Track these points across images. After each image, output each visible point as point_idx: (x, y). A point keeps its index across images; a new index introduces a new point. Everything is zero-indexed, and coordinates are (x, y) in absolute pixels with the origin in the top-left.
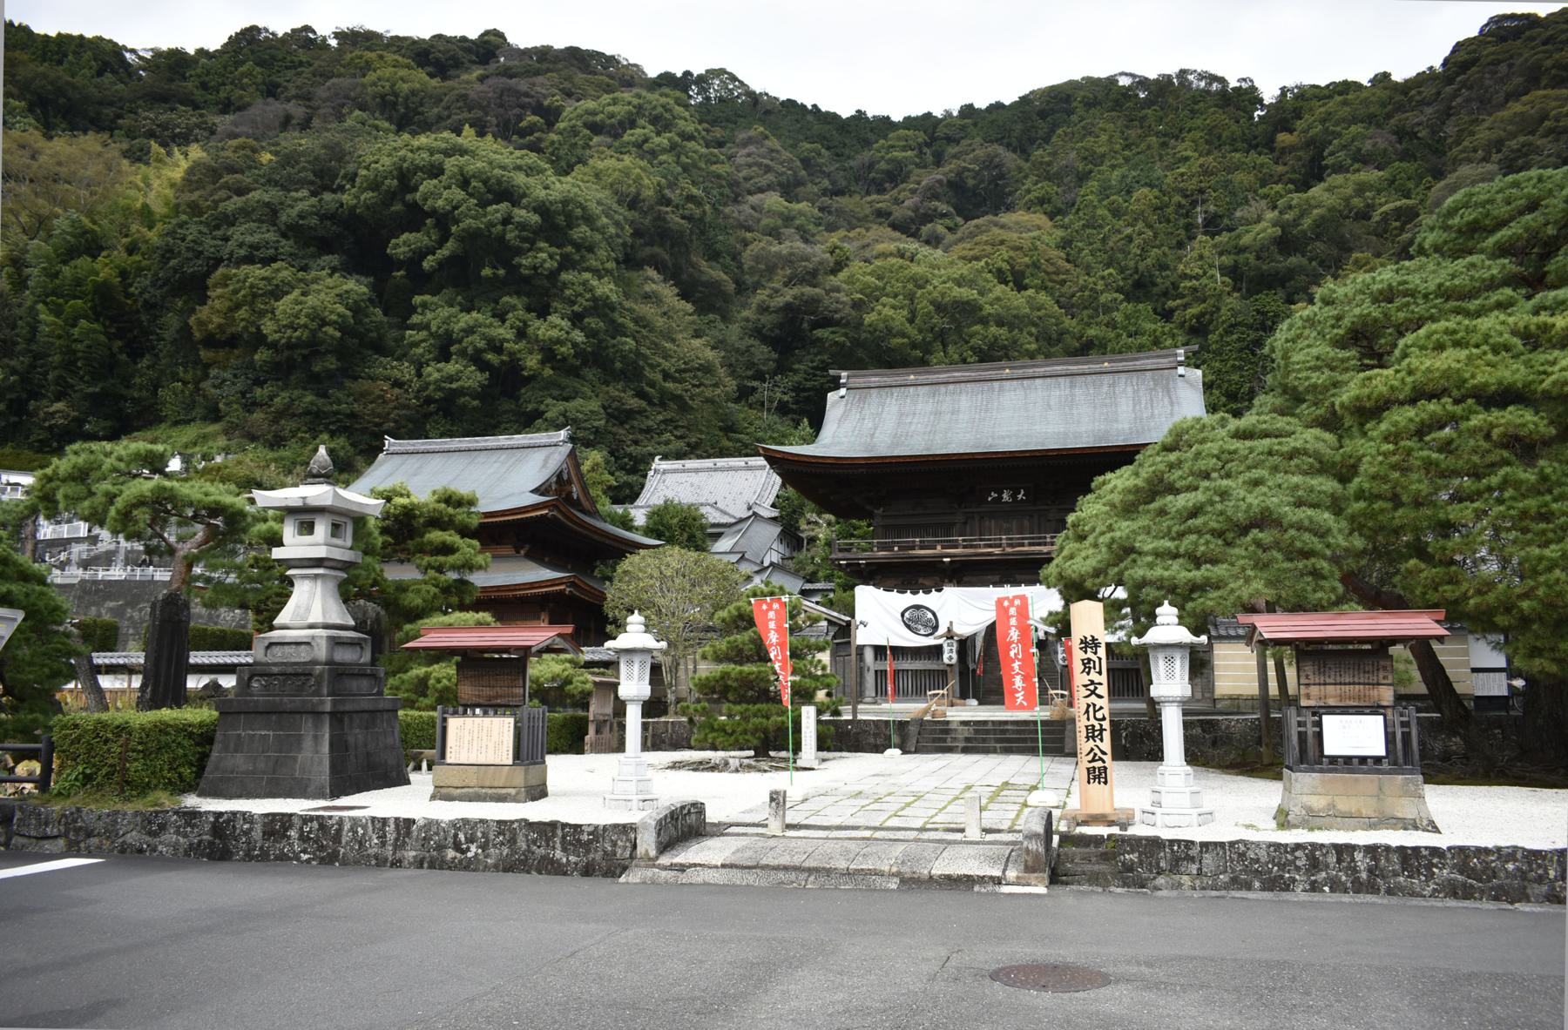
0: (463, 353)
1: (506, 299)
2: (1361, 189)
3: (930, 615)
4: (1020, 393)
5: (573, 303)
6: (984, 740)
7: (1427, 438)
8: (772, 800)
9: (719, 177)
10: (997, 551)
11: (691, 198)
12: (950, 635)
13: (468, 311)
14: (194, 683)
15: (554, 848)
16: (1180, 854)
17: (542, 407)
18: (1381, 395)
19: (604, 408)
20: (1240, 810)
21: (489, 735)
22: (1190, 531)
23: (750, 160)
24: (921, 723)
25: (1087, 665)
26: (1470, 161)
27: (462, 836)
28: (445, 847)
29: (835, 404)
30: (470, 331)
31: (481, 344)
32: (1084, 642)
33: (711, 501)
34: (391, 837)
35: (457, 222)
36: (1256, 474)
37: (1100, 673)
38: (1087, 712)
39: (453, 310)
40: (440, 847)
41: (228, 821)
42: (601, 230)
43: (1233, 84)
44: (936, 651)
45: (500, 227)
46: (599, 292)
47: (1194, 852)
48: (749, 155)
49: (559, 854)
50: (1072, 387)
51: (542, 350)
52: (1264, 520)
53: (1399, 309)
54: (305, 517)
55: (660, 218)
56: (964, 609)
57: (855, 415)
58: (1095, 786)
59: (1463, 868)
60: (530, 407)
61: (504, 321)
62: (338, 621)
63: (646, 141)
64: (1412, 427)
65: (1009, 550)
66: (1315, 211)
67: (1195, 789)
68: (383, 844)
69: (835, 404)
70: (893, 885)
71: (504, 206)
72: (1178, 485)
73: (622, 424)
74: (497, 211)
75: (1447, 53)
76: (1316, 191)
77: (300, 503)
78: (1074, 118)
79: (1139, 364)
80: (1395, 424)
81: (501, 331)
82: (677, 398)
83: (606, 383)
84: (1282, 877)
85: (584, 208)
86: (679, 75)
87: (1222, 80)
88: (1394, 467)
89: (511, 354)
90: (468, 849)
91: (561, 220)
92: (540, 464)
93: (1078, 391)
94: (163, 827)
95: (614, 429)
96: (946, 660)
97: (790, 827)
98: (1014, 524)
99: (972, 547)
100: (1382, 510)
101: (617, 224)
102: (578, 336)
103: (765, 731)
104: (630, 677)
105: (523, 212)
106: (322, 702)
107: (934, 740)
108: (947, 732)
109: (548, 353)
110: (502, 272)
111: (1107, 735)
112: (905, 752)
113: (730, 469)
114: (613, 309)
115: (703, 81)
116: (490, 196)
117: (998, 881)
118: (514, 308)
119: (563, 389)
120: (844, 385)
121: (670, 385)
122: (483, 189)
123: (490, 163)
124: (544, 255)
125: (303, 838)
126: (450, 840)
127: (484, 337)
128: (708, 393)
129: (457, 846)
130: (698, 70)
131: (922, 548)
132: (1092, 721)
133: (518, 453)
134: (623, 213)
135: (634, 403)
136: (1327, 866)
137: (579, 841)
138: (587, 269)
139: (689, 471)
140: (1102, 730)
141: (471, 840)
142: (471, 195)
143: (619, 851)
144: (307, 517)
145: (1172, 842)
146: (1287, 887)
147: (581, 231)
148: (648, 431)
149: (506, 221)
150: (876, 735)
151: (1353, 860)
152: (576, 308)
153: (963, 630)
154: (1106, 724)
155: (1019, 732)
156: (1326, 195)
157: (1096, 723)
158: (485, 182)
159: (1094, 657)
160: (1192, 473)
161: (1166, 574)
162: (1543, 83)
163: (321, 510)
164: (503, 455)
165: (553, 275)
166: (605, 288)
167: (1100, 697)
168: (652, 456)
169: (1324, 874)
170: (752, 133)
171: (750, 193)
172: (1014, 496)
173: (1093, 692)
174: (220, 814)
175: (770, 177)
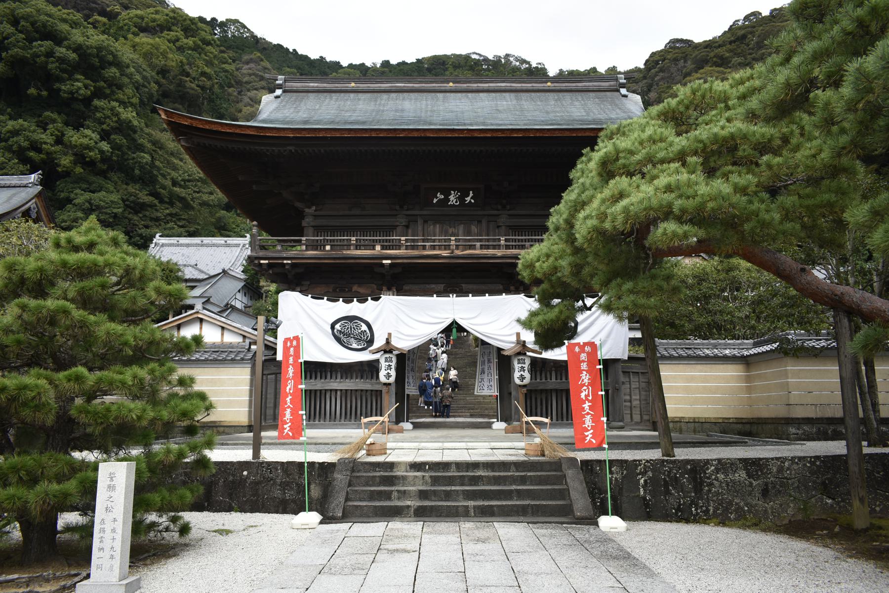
1: (47, 113)
3: (364, 327)
5: (104, 123)
6: (448, 495)
9: (226, 71)
10: (445, 253)
11: (204, 74)
12: (388, 349)
17: (72, 196)
19: (123, 200)
23: (250, 71)
24: (353, 466)
29: (267, 104)
30: (15, 133)
31: (26, 144)
33: (193, 263)
35: (6, 49)
42: (130, 76)
43: (534, 65)
44: (371, 368)
45: (43, 58)
46: (124, 116)
48: (250, 69)
51: (75, 154)
55: (181, 84)
56: (406, 320)
60: (62, 195)
61: (45, 130)
63: (178, 40)
65: (458, 253)
71: (48, 43)
73: (136, 213)
74: (41, 46)
75: (647, 57)
78: (447, 73)
81: (43, 136)
82: (182, 199)
83: (127, 184)
86: (209, 19)
87: (528, 63)
89: (48, 154)
95: (130, 216)
96: (382, 378)
98: (461, 228)
99: (413, 248)
101: (144, 78)
102: (105, 146)
105: (63, 50)
107: (373, 496)
108: (391, 481)
109: (80, 158)
110: (45, 93)
112: (327, 519)
113: (214, 245)
114: (135, 132)
115: (223, 25)
116: (37, 36)
118: (54, 121)
119: (90, 184)
120: (279, 87)
122: (30, 28)
123: (38, 11)
124: (80, 84)
127: (27, 139)
128: (205, 197)
130: (221, 18)
131: (357, 247)
138: (117, 100)
139: (182, 245)
142: (21, 32)
147: (113, 71)
148: (157, 219)
149: (50, 54)
150: (284, 486)
152: (104, 126)
153: (403, 343)
155: (497, 480)
158: (33, 24)
165: (87, 101)
166: (128, 114)
170: (252, 56)
171: (249, 90)
172: (461, 199)
175: (263, 83)
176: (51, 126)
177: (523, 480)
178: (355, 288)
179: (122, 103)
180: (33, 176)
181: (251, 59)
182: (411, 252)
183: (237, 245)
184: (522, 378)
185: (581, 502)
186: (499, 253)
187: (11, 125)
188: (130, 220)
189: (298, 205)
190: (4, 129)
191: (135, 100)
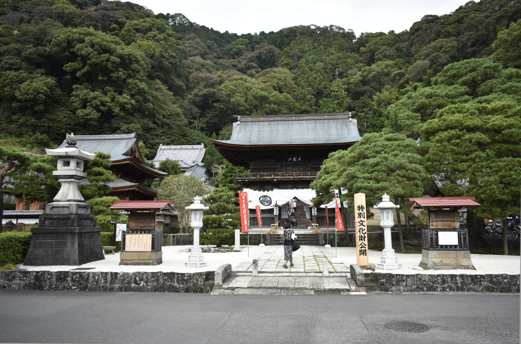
0: (92, 106)
1: (107, 87)
2: (387, 66)
3: (269, 199)
4: (299, 125)
5: (132, 90)
7: (451, 142)
8: (254, 263)
9: (180, 50)
10: (292, 177)
11: (172, 56)
12: (276, 205)
13: (94, 91)
14: (4, 222)
15: (174, 282)
16: (400, 279)
17: (120, 126)
18: (435, 128)
19: (142, 127)
20: (407, 264)
21: (142, 241)
22: (375, 171)
23: (190, 45)
24: (271, 235)
25: (360, 215)
26: (420, 59)
27: (138, 279)
28: (131, 283)
29: (236, 127)
30: (94, 98)
31: (99, 103)
32: (359, 207)
33: (181, 160)
34: (109, 279)
35: (89, 59)
36: (395, 152)
37: (364, 218)
38: (360, 231)
39: (88, 91)
40: (129, 283)
41: (42, 275)
42: (141, 66)
43: (347, 31)
44: (271, 211)
45: (105, 62)
46: (141, 87)
47: (404, 278)
48: (190, 43)
49: (176, 284)
50: (316, 123)
51: (120, 106)
52: (401, 167)
53: (434, 101)
54: (66, 159)
55: (161, 62)
56: (281, 197)
57: (243, 131)
58: (362, 256)
59: (491, 282)
60: (115, 126)
61: (106, 95)
62: (79, 199)
63: (156, 36)
64: (447, 138)
65: (296, 177)
66: (373, 73)
67: (396, 257)
68: (106, 282)
69: (236, 127)
70: (313, 293)
71: (107, 55)
72: (369, 155)
73: (148, 132)
74: (105, 57)
75: (411, 26)
76: (373, 66)
77: (65, 154)
78: (297, 38)
79: (337, 117)
80: (441, 137)
81: (106, 99)
82: (168, 125)
84: (433, 286)
85: (136, 58)
86: (165, 14)
87: (343, 29)
88: (441, 151)
89: (109, 107)
90: (140, 283)
91: (127, 61)
92: (125, 145)
93: (317, 125)
94: (14, 278)
95: (145, 134)
97: (260, 272)
99: (283, 176)
100: (437, 165)
101: (146, 64)
102: (133, 102)
103: (222, 238)
104: (195, 219)
105: (114, 58)
106: (75, 229)
107: (275, 241)
108: (280, 238)
109: (123, 107)
110: (105, 78)
111: (366, 239)
112: (266, 245)
113: (187, 149)
114: (145, 93)
115: (174, 17)
116: (102, 51)
117: (348, 290)
118: (110, 91)
119: (127, 120)
120: (239, 121)
121: (165, 120)
122: (99, 49)
123: (102, 39)
124: (121, 73)
125: (73, 280)
126: (133, 280)
127: (100, 101)
128: (178, 123)
129: (136, 282)
130: (172, 13)
131: (267, 176)
132: (361, 234)
133: (117, 141)
134: (148, 60)
135: (152, 125)
136: (448, 282)
137: (184, 279)
138: (136, 79)
139: (172, 149)
140: (365, 237)
141: (141, 280)
142: (95, 50)
143: (199, 283)
144: (67, 160)
145: (397, 275)
146: (435, 290)
147: (135, 66)
148: (157, 135)
149: (108, 60)
150: (255, 239)
151: (456, 280)
152: (132, 92)
153: (280, 203)
154: (366, 235)
155: (303, 238)
156: (376, 67)
157: (363, 235)
158: (100, 46)
159: (362, 212)
160: (373, 152)
161: (369, 185)
162: (441, 37)
163: (73, 157)
164: (111, 142)
165: (124, 80)
166: (143, 85)
167: (364, 226)
168: (159, 144)
169: (447, 285)
170: (191, 36)
171: (190, 56)
172: (297, 159)
173: (362, 224)
174: (38, 272)
175: (197, 51)
176: (108, 93)
177: (309, 238)
178: (266, 187)
179: (139, 80)
180: (133, 134)
181: (190, 38)
182: (282, 177)
183: (198, 149)
184: (314, 213)
185: (322, 241)
186: (308, 177)
187: (92, 94)
188: (145, 136)
189: (248, 162)
190: (89, 97)
191: (145, 78)
